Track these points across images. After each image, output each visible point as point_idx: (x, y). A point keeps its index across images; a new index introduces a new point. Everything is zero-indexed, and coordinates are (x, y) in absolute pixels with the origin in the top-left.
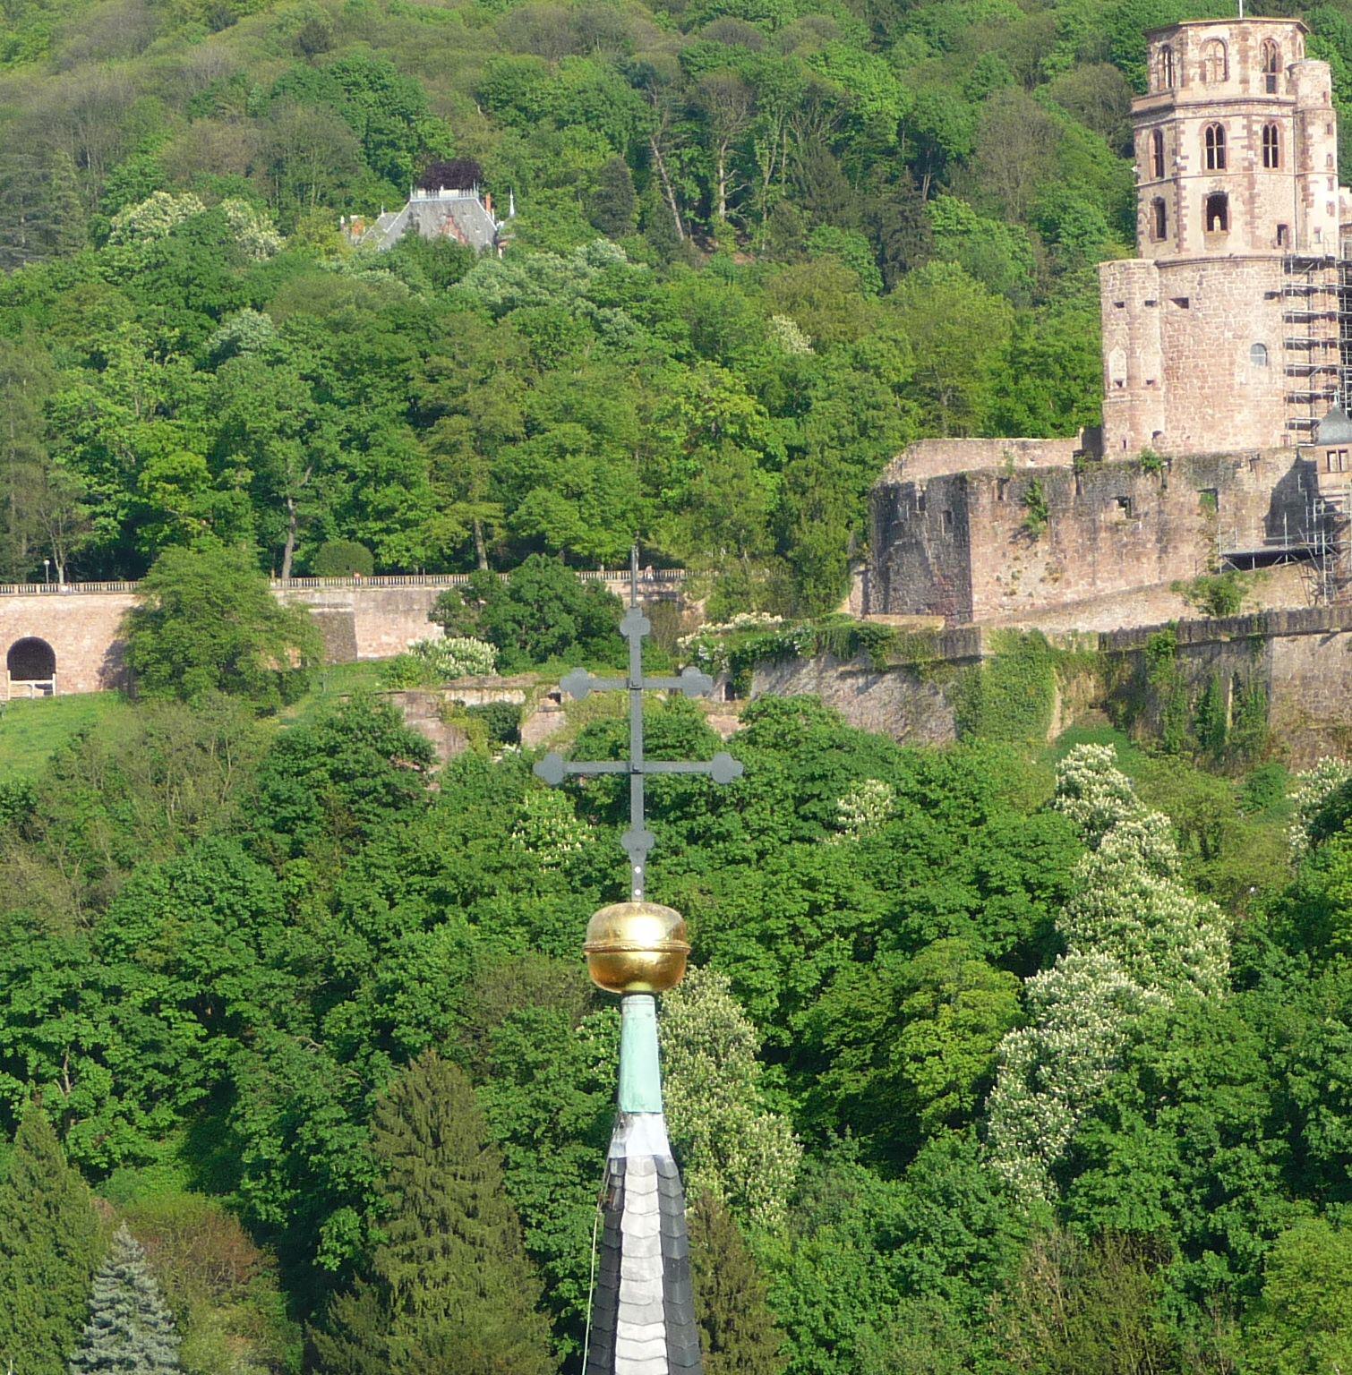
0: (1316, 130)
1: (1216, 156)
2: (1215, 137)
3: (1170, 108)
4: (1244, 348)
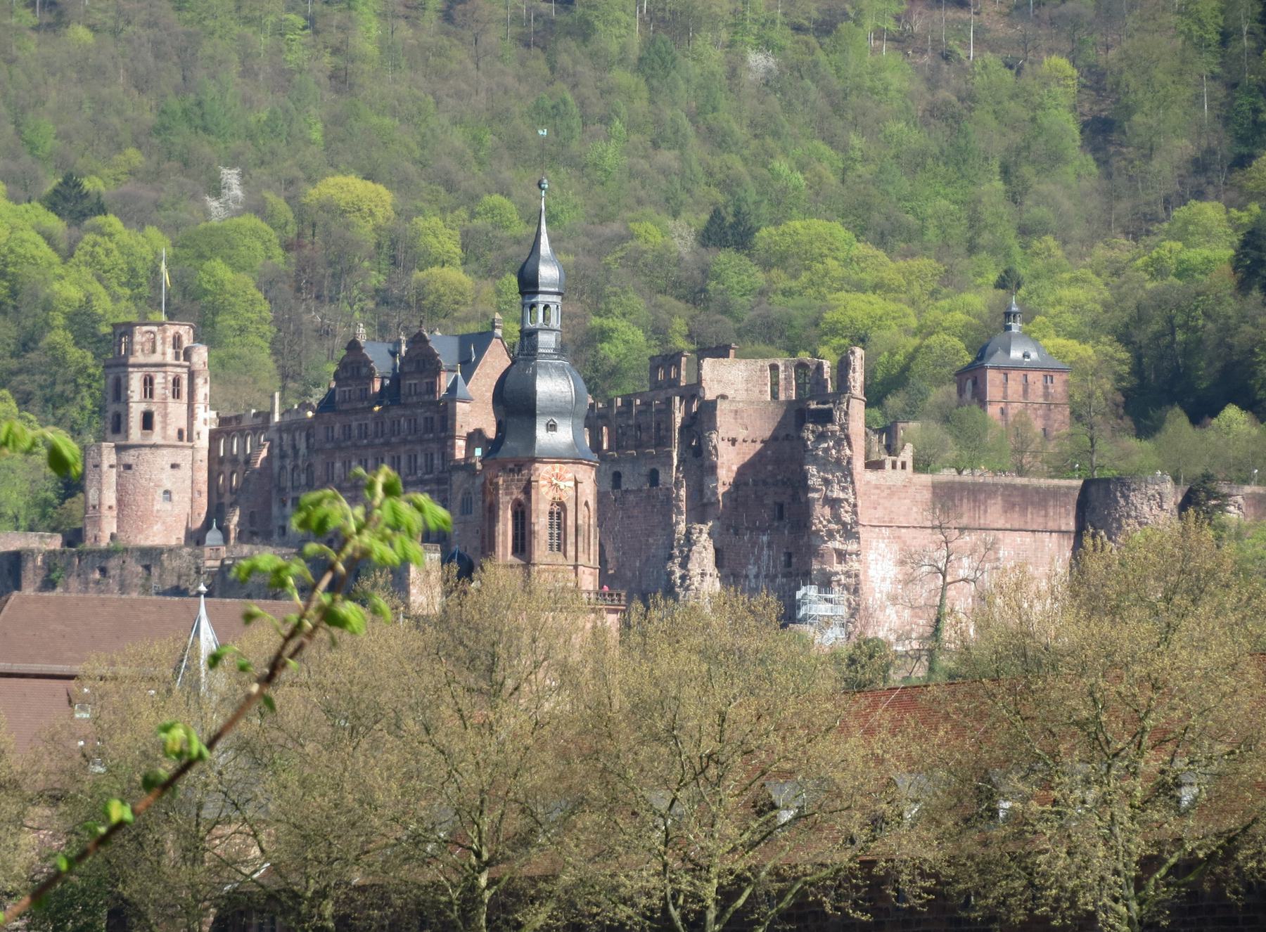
0: (199, 381)
2: (148, 382)
4: (160, 491)
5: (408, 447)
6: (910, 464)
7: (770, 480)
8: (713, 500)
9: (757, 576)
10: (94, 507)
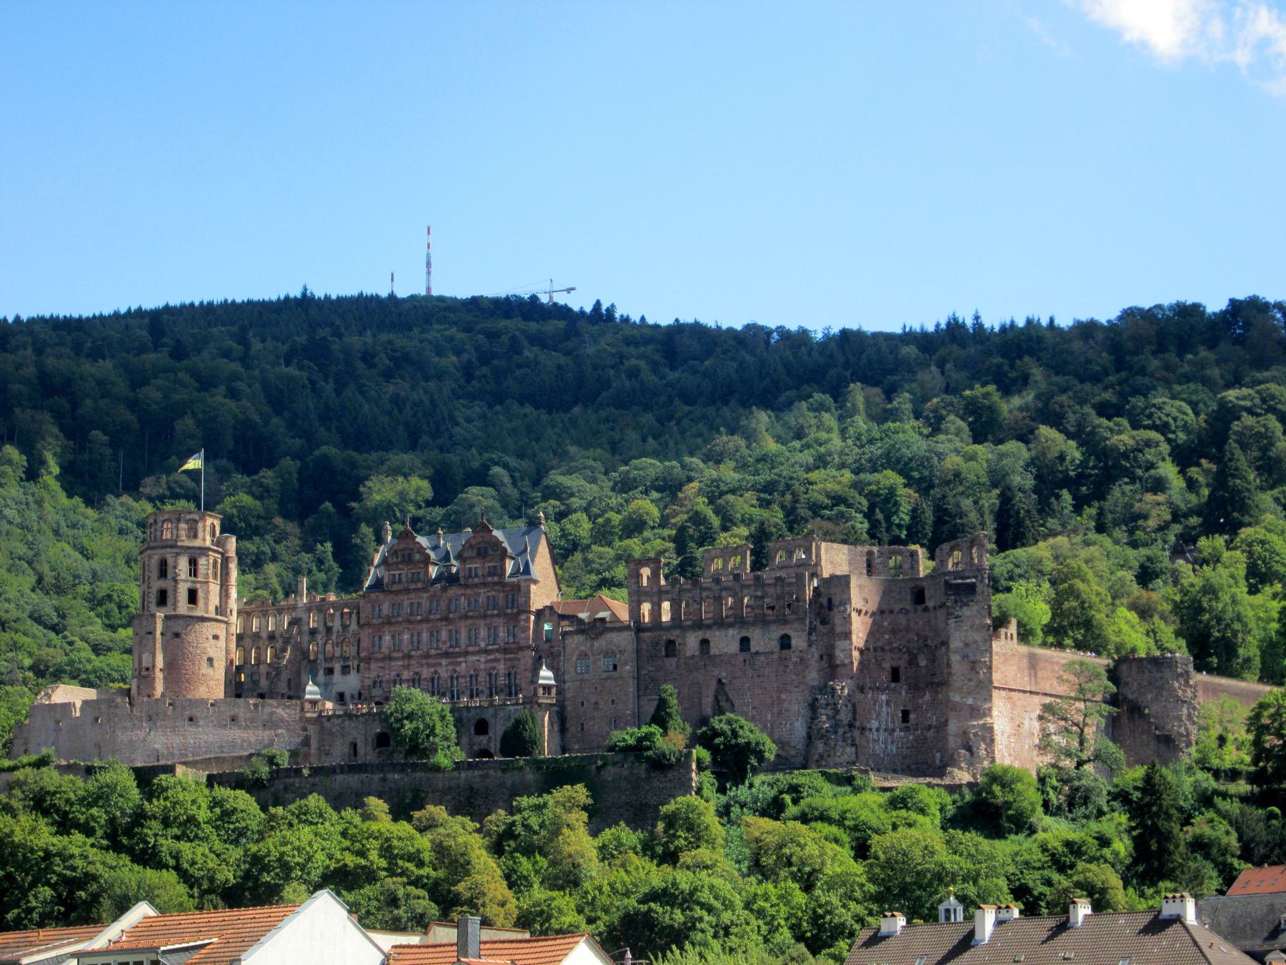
1: (194, 572)
2: (193, 563)
5: (469, 622)
6: (1015, 636)
7: (887, 648)
8: (847, 661)
9: (878, 730)
10: (147, 669)
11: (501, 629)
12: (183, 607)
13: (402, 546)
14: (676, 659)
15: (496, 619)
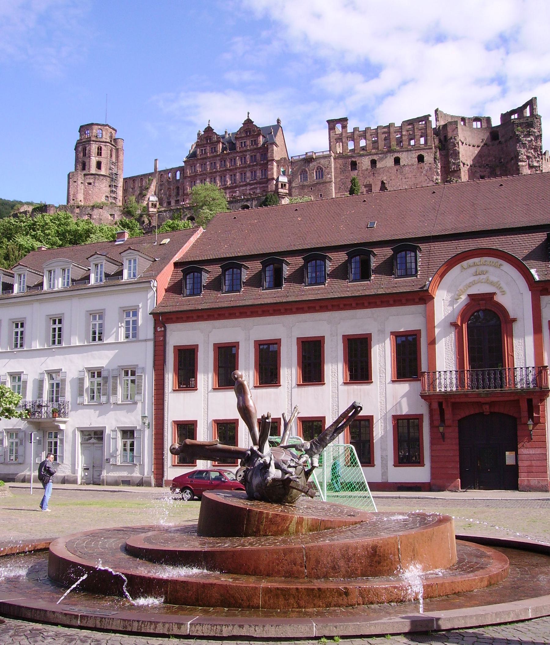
1: (99, 154)
2: (100, 149)
3: (90, 141)
7: (477, 165)
11: (258, 172)
12: (93, 170)
13: (206, 135)
14: (357, 171)
15: (255, 167)
